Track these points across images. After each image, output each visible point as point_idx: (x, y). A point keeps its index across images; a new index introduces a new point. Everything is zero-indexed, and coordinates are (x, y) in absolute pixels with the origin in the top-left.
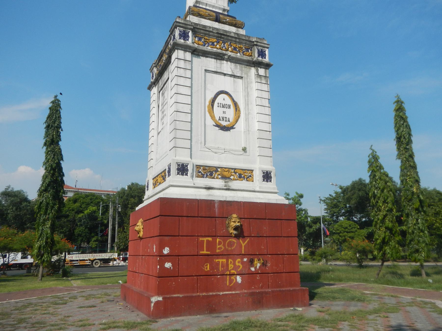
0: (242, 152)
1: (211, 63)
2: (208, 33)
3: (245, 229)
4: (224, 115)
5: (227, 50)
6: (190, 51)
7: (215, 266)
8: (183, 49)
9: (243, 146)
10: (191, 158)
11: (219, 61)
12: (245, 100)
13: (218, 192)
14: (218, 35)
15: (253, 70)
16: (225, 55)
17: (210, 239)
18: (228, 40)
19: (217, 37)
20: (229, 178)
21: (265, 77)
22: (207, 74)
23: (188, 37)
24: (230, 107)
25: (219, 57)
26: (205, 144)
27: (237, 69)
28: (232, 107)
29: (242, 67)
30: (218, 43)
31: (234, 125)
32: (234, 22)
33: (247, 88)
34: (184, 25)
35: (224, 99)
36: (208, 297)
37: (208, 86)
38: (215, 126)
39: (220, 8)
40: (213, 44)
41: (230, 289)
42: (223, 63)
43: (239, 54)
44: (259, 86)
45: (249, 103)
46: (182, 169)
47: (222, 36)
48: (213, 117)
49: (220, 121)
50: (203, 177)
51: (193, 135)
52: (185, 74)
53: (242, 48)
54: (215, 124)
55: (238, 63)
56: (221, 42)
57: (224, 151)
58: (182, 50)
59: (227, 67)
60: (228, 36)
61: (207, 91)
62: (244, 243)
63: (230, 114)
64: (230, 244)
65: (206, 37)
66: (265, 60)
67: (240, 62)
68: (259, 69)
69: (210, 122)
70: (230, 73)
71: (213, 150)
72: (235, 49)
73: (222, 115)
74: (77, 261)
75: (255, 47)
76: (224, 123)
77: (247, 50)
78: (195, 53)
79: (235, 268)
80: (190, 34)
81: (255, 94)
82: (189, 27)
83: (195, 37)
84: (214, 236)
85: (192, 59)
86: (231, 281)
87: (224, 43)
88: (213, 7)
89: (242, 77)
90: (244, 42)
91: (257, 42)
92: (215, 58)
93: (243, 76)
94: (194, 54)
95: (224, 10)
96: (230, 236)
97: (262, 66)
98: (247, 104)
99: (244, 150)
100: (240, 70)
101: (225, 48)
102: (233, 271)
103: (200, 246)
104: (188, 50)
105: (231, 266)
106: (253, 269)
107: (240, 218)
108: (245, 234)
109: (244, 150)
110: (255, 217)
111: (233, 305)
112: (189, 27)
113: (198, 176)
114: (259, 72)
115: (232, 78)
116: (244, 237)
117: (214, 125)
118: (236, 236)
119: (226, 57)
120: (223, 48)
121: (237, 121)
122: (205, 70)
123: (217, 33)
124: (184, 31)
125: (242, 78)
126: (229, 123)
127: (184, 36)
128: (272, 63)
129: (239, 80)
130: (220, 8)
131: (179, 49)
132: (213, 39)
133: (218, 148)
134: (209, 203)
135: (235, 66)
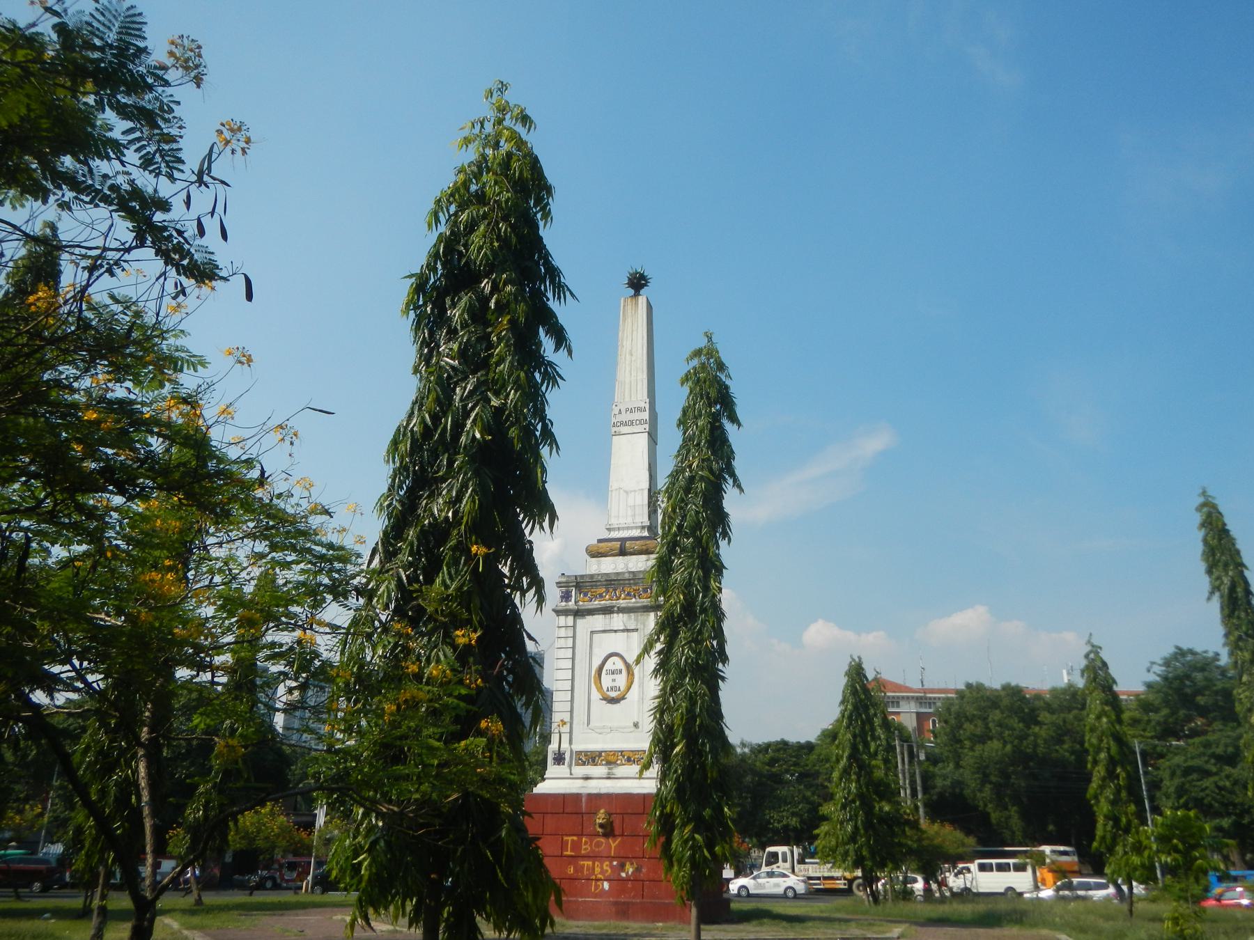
0: (633, 729)
1: (598, 621)
3: (617, 824)
5: (618, 599)
7: (579, 869)
13: (598, 782)
20: (615, 763)
24: (621, 672)
25: (607, 611)
28: (624, 672)
30: (607, 592)
37: (595, 650)
40: (601, 595)
41: (596, 896)
46: (559, 759)
47: (612, 583)
48: (600, 688)
50: (584, 764)
59: (618, 620)
61: (594, 659)
62: (614, 843)
63: (621, 681)
64: (599, 845)
69: (596, 695)
72: (629, 594)
73: (611, 684)
74: (819, 878)
76: (613, 694)
77: (645, 590)
79: (603, 872)
84: (581, 835)
86: (597, 887)
87: (615, 590)
95: (643, 528)
96: (597, 835)
102: (600, 876)
103: (563, 846)
105: (597, 870)
106: (623, 875)
107: (610, 814)
109: (636, 725)
111: (592, 913)
113: (577, 764)
116: (614, 836)
118: (605, 835)
121: (629, 688)
134: (576, 797)
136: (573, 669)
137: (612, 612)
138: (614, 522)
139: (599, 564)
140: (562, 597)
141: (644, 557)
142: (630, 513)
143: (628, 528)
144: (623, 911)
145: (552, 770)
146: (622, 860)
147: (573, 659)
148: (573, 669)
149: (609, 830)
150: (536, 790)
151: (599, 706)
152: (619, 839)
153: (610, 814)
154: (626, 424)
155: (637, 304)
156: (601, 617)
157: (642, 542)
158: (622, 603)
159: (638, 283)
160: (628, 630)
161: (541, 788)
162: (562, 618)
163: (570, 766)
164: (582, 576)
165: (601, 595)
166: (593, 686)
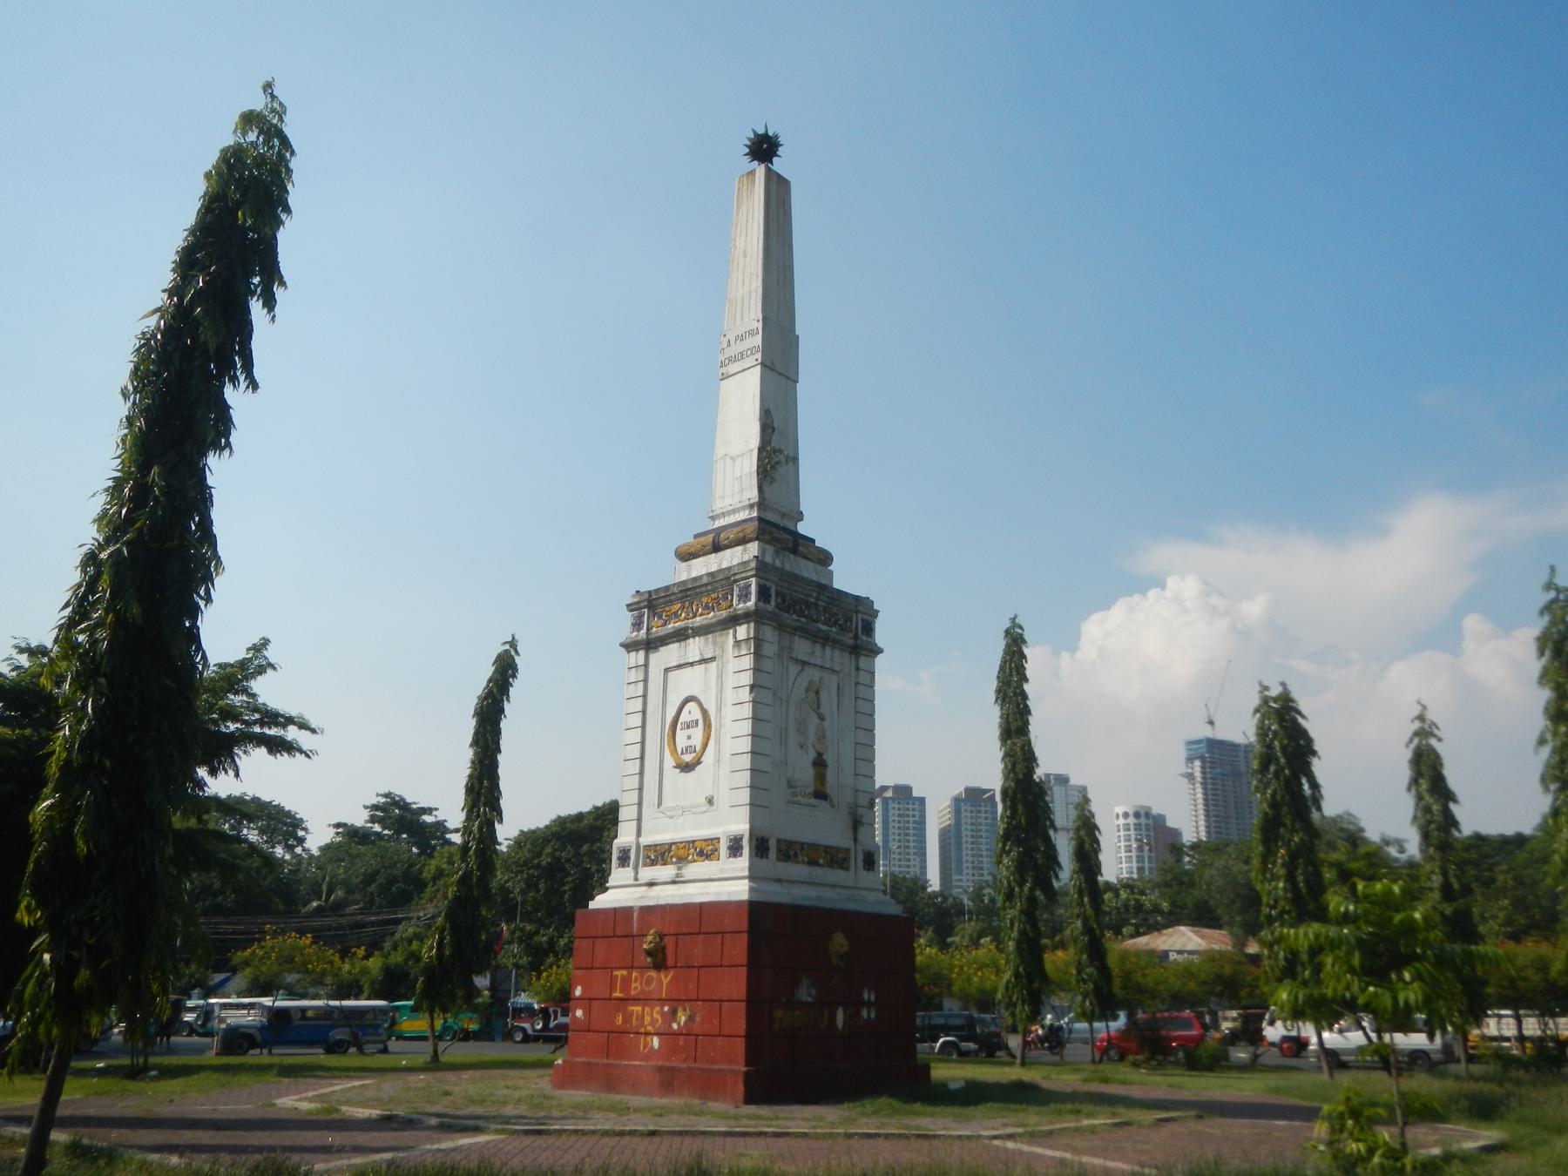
1: (670, 654)
3: (670, 952)
9: (709, 793)
10: (639, 834)
16: (686, 629)
17: (625, 972)
22: (671, 675)
25: (681, 636)
28: (701, 723)
33: (720, 676)
36: (607, 1066)
39: (743, 508)
41: (645, 1057)
46: (624, 860)
47: (688, 593)
50: (653, 863)
59: (695, 648)
62: (666, 978)
63: (697, 734)
69: (669, 762)
70: (698, 658)
76: (688, 758)
81: (731, 681)
85: (647, 658)
86: (646, 1045)
88: (734, 511)
95: (751, 506)
98: (719, 709)
99: (710, 801)
102: (650, 1028)
105: (647, 1019)
107: (662, 936)
108: (670, 962)
109: (710, 801)
110: (684, 930)
116: (667, 968)
125: (713, 659)
130: (743, 508)
136: (643, 727)
137: (687, 638)
138: (719, 506)
139: (689, 568)
140: (634, 625)
141: (739, 548)
142: (737, 489)
143: (734, 511)
144: (668, 1080)
145: (618, 875)
146: (675, 1001)
147: (644, 712)
148: (643, 727)
149: (658, 959)
150: (592, 905)
152: (671, 973)
153: (662, 936)
154: (732, 360)
155: (753, 181)
156: (676, 645)
157: (736, 530)
158: (698, 621)
159: (764, 148)
160: (704, 661)
161: (600, 902)
162: (633, 654)
163: (636, 868)
164: (657, 591)
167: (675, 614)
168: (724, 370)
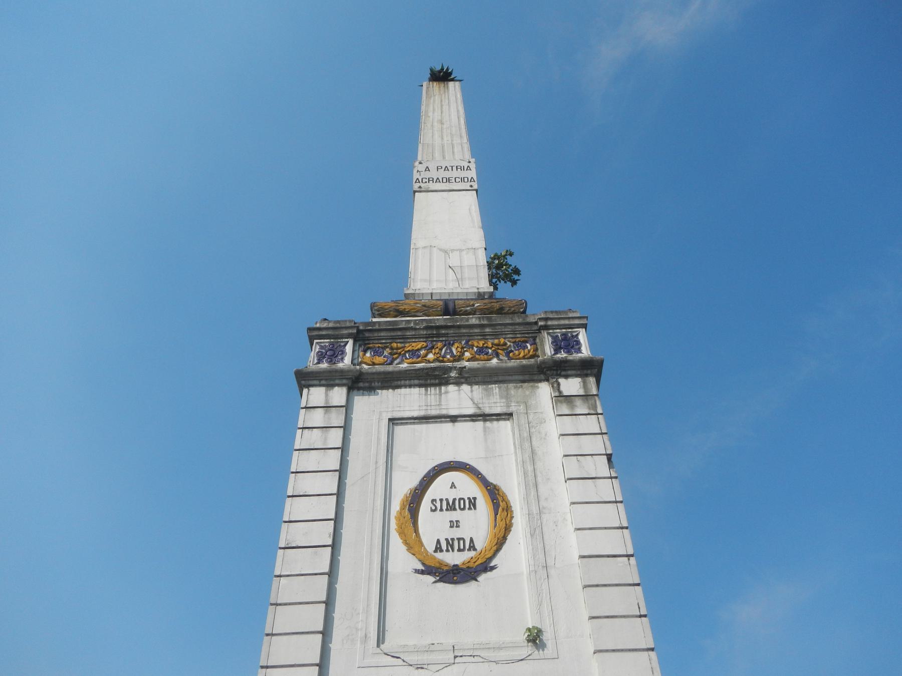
0: (528, 649)
1: (411, 400)
2: (399, 333)
4: (455, 533)
5: (459, 358)
6: (344, 381)
8: (323, 382)
11: (432, 390)
12: (525, 474)
14: (429, 332)
15: (544, 390)
18: (461, 336)
19: (427, 337)
21: (586, 397)
22: (399, 430)
23: (343, 353)
24: (473, 503)
25: (433, 378)
26: (380, 640)
27: (492, 399)
29: (507, 389)
31: (491, 559)
32: (497, 306)
34: (330, 332)
35: (453, 486)
37: (401, 458)
38: (422, 572)
42: (446, 392)
43: (495, 361)
44: (569, 425)
45: (539, 479)
48: (413, 544)
49: (439, 555)
51: (337, 615)
52: (326, 439)
53: (505, 344)
54: (421, 567)
55: (495, 382)
56: (440, 345)
57: (451, 656)
58: (320, 385)
59: (458, 398)
60: (459, 327)
61: (396, 475)
63: (477, 525)
65: (394, 345)
66: (580, 355)
67: (501, 378)
68: (562, 381)
69: (402, 561)
70: (471, 411)
71: (409, 658)
72: (481, 350)
75: (545, 334)
77: (521, 345)
78: (361, 385)
80: (349, 348)
82: (345, 332)
83: (365, 351)
87: (449, 345)
89: (511, 415)
90: (510, 328)
91: (546, 319)
92: (420, 386)
93: (513, 409)
94: (359, 389)
97: (570, 372)
98: (533, 483)
99: (535, 638)
100: (501, 397)
101: (453, 355)
104: (337, 382)
109: (535, 638)
112: (345, 332)
114: (562, 388)
115: (480, 424)
117: (417, 571)
119: (453, 374)
120: (444, 357)
121: (500, 543)
122: (390, 420)
123: (426, 328)
124: (331, 343)
125: (509, 416)
126: (472, 554)
127: (334, 354)
128: (599, 357)
129: (502, 423)
131: (313, 386)
132: (414, 344)
133: (430, 649)
135: (486, 390)
137: (447, 383)
148: (340, 495)
151: (411, 591)
156: (416, 391)
160: (485, 417)
165: (414, 353)
166: (396, 541)
167: (414, 353)
168: (422, 185)
